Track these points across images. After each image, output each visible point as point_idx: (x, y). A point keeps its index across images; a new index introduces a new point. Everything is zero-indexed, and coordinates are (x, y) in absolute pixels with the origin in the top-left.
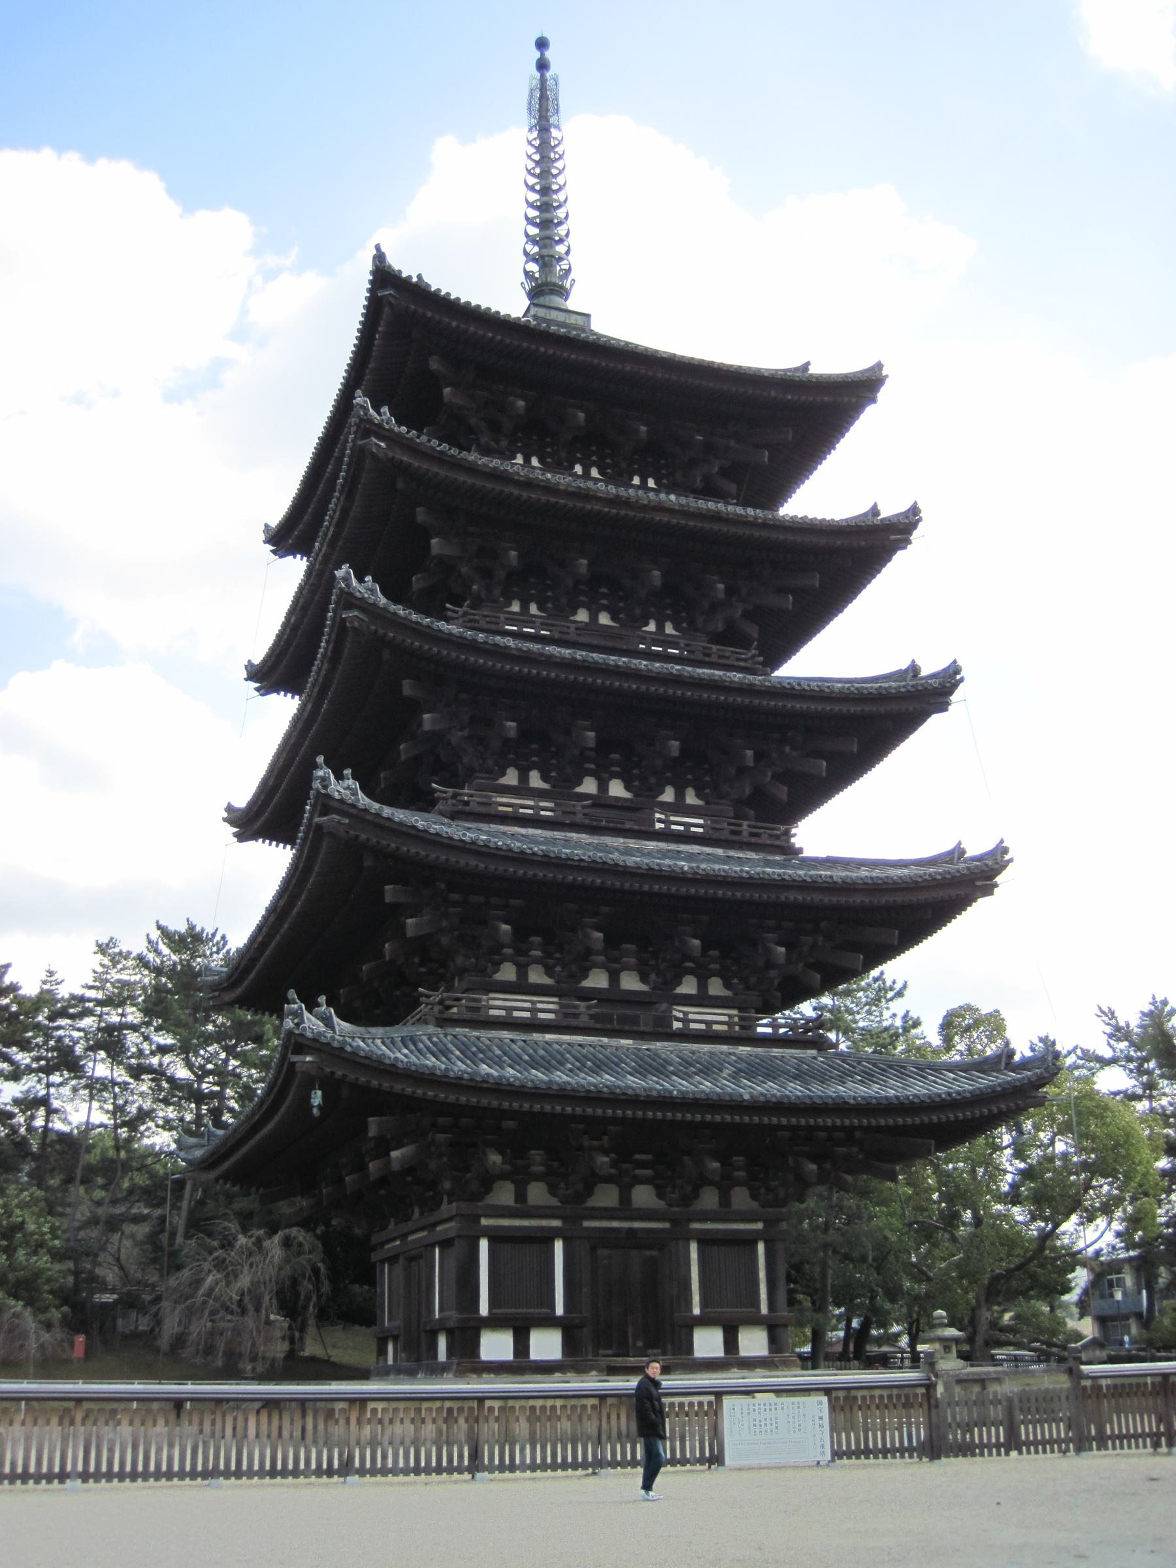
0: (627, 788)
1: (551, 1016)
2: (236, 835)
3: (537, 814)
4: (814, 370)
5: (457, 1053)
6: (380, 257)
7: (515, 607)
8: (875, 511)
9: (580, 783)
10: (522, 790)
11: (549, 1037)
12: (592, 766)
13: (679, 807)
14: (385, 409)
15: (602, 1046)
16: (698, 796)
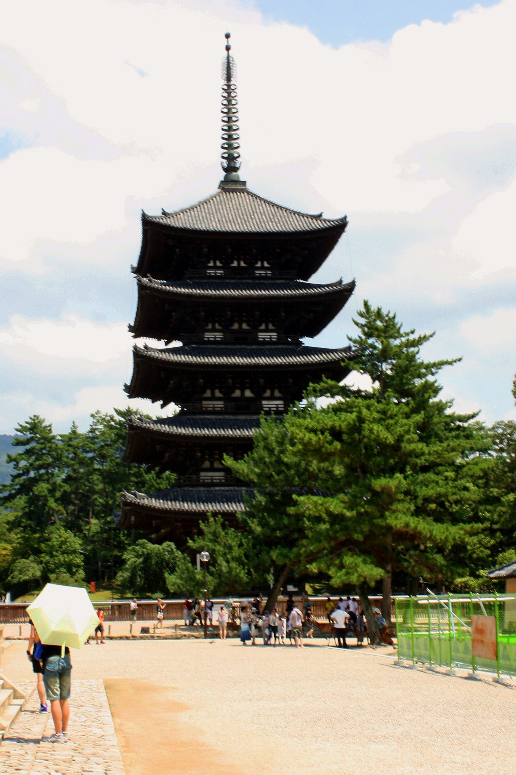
0: (252, 392)
1: (218, 481)
2: (128, 396)
3: (214, 410)
4: (324, 216)
5: (180, 499)
6: (144, 215)
7: (210, 326)
8: (340, 282)
9: (233, 392)
10: (213, 398)
11: (217, 488)
12: (238, 385)
13: (272, 398)
14: (149, 275)
15: (235, 491)
16: (280, 392)
